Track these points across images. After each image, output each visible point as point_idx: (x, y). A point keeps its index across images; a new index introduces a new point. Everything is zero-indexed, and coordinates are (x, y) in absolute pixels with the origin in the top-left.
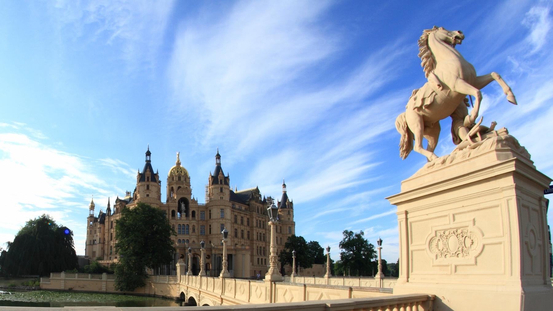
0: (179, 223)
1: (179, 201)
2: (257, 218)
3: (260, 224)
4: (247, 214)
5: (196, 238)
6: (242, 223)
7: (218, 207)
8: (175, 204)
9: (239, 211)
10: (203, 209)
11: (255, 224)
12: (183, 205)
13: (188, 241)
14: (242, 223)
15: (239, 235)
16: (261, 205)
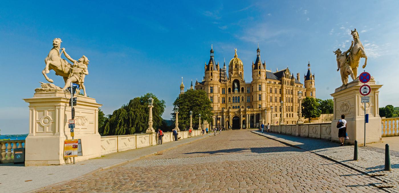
0: (233, 96)
1: (233, 82)
2: (287, 88)
3: (289, 92)
4: (280, 86)
5: (244, 105)
6: (276, 92)
7: (257, 84)
8: (230, 84)
9: (273, 85)
10: (249, 86)
11: (284, 92)
12: (236, 85)
13: (239, 107)
14: (276, 92)
15: (273, 100)
16: (290, 80)
